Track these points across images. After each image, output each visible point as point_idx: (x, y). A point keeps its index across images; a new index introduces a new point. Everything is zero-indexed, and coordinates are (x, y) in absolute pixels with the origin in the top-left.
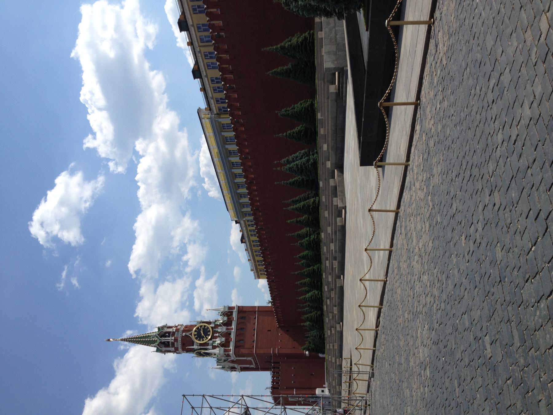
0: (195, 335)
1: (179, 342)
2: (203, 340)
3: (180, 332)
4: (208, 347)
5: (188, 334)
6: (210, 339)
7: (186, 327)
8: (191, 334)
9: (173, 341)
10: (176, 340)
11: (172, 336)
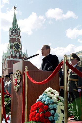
2: (14, 47)
4: (11, 48)
5: (17, 40)
6: (14, 50)
7: (20, 40)
8: (17, 42)
9: (14, 34)
11: (16, 34)
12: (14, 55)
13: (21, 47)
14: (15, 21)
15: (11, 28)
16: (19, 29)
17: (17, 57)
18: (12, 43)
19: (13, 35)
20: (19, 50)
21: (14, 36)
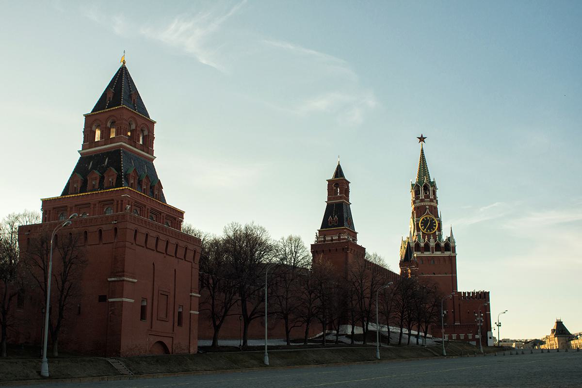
0: (426, 218)
1: (420, 204)
3: (428, 203)
5: (428, 210)
6: (423, 232)
7: (436, 208)
8: (428, 214)
10: (422, 201)
12: (422, 245)
13: (440, 224)
14: (424, 167)
15: (414, 184)
16: (433, 184)
17: (431, 247)
18: (416, 218)
19: (419, 200)
20: (434, 231)
21: (422, 201)
